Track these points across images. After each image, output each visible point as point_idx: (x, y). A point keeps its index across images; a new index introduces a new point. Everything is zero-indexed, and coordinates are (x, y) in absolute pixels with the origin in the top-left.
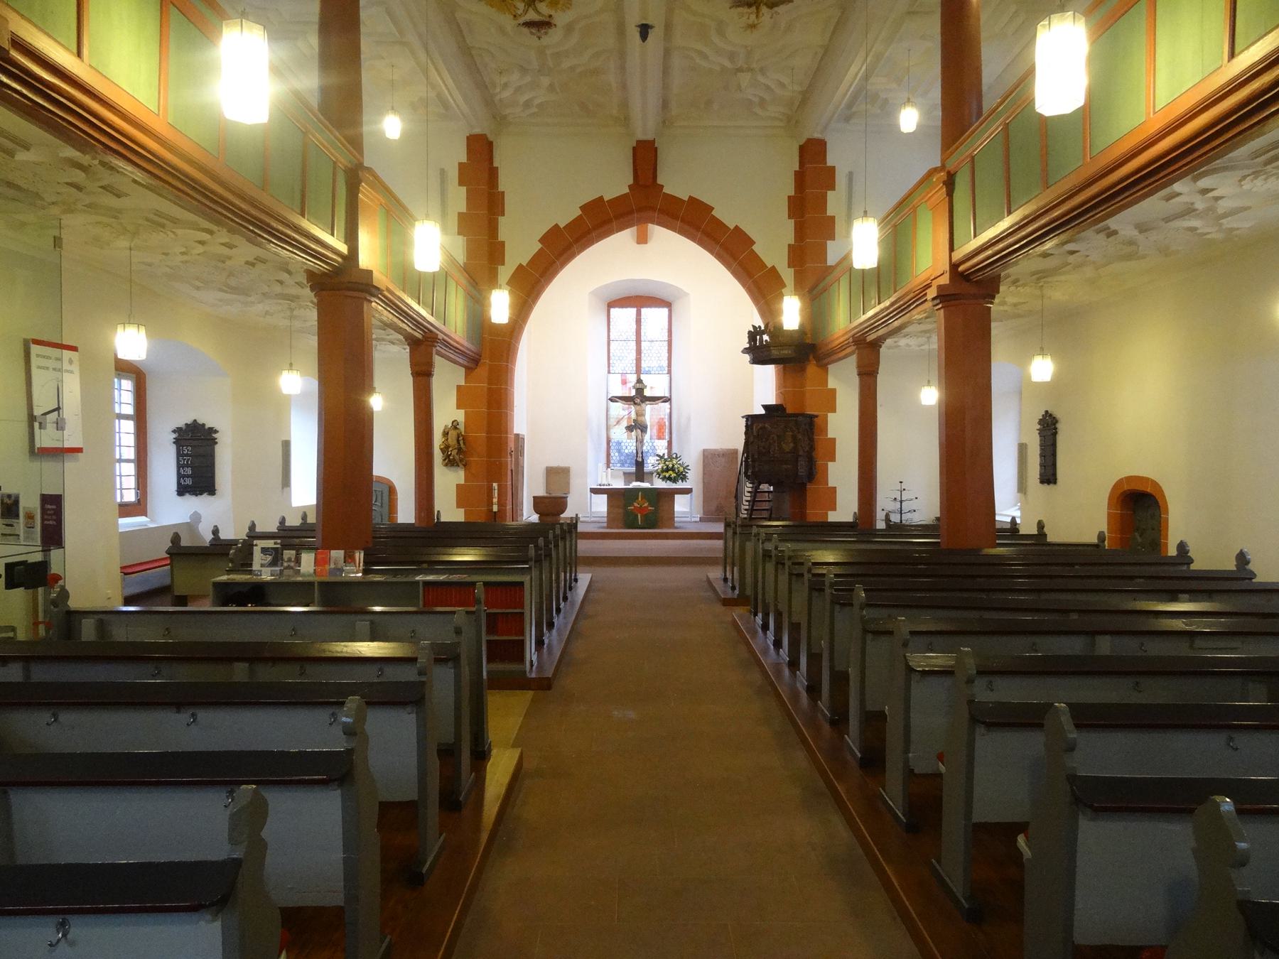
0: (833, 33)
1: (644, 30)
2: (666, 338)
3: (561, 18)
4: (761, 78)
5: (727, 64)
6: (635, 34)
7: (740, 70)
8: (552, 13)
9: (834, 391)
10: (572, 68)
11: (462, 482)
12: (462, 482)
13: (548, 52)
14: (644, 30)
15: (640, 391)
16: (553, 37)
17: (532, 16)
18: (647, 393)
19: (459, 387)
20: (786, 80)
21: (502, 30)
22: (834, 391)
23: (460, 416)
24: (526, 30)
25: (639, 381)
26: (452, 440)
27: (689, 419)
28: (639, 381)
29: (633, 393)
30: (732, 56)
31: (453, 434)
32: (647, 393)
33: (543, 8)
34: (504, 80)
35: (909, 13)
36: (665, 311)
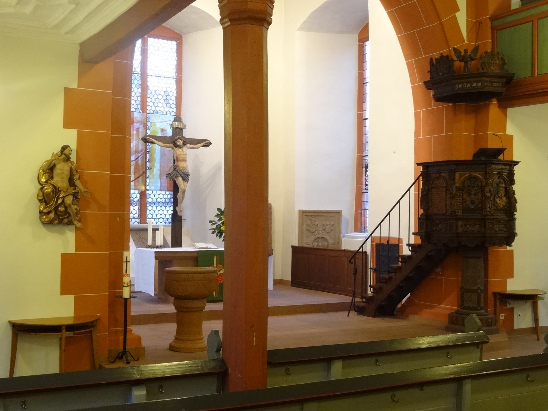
2: (174, 75)
9: (511, 137)
11: (71, 250)
12: (71, 250)
15: (178, 131)
18: (187, 134)
19: (67, 91)
22: (511, 137)
23: (70, 138)
25: (178, 118)
26: (60, 180)
28: (178, 118)
29: (169, 133)
31: (62, 169)
32: (187, 134)
36: (172, 45)
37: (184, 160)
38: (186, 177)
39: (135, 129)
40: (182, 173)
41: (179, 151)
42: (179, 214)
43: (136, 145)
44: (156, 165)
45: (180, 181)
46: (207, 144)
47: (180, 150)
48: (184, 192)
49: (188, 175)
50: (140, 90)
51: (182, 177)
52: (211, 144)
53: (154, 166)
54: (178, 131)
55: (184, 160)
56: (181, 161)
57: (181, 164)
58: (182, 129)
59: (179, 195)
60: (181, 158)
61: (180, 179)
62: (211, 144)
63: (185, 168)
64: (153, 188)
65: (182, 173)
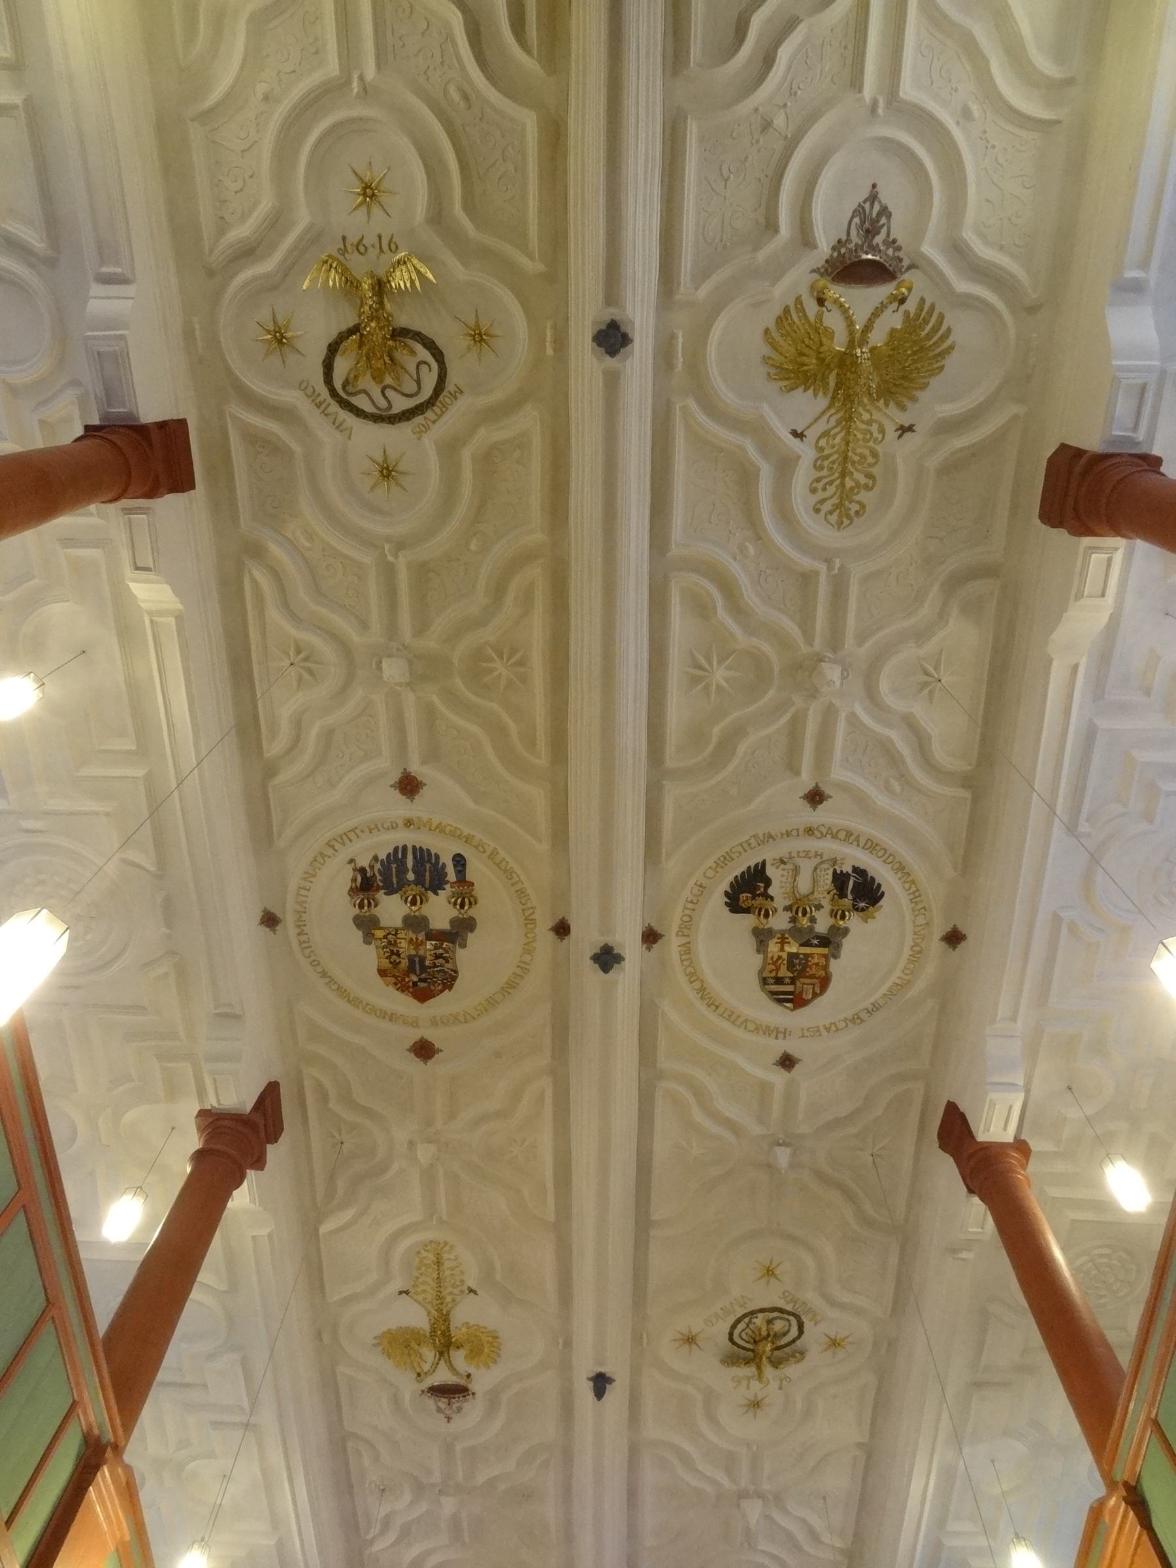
0: (873, 1423)
1: (601, 1383)
3: (483, 1381)
4: (777, 1515)
5: (726, 1482)
6: (585, 1390)
7: (743, 1495)
8: (471, 1370)
10: (491, 1483)
13: (459, 1447)
14: (601, 1383)
16: (472, 1411)
17: (443, 1376)
20: (817, 1523)
21: (396, 1401)
24: (430, 1402)
30: (729, 1463)
33: (459, 1357)
34: (384, 1510)
35: (978, 1385)
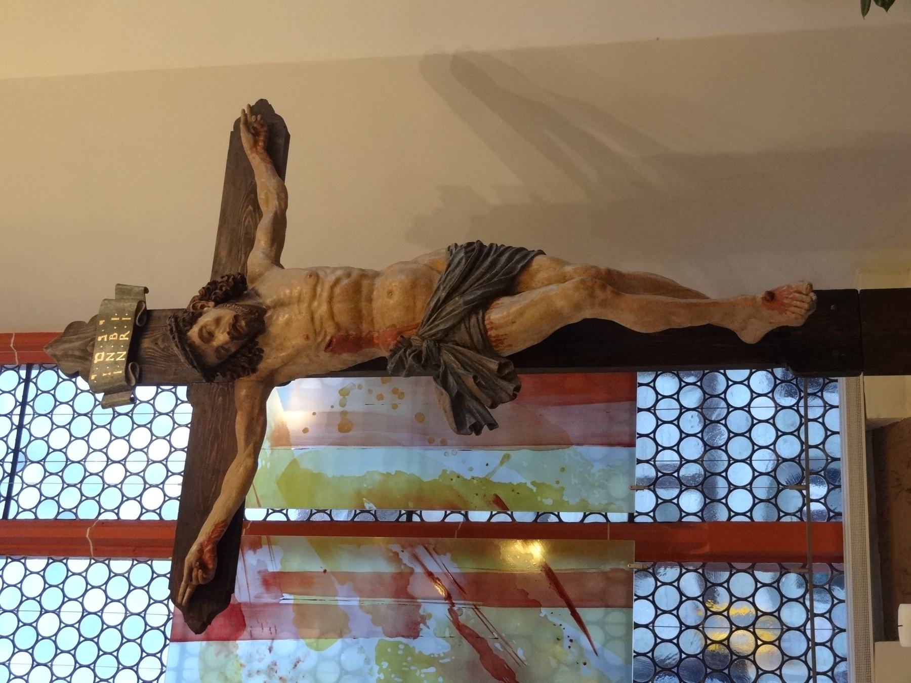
27: (472, 79)
37: (356, 288)
38: (487, 270)
39: (267, 599)
40: (458, 303)
41: (287, 329)
42: (793, 316)
43: (360, 592)
44: (479, 473)
45: (512, 319)
46: (264, 134)
47: (279, 321)
48: (613, 282)
49: (476, 253)
50: (77, 564)
51: (485, 303)
52: (262, 108)
53: (486, 481)
54: (155, 345)
55: (358, 286)
56: (358, 316)
57: (389, 309)
58: (148, 314)
59: (628, 315)
60: (338, 307)
61: (501, 313)
62: (262, 108)
63: (417, 281)
64: (619, 487)
65: (458, 303)
